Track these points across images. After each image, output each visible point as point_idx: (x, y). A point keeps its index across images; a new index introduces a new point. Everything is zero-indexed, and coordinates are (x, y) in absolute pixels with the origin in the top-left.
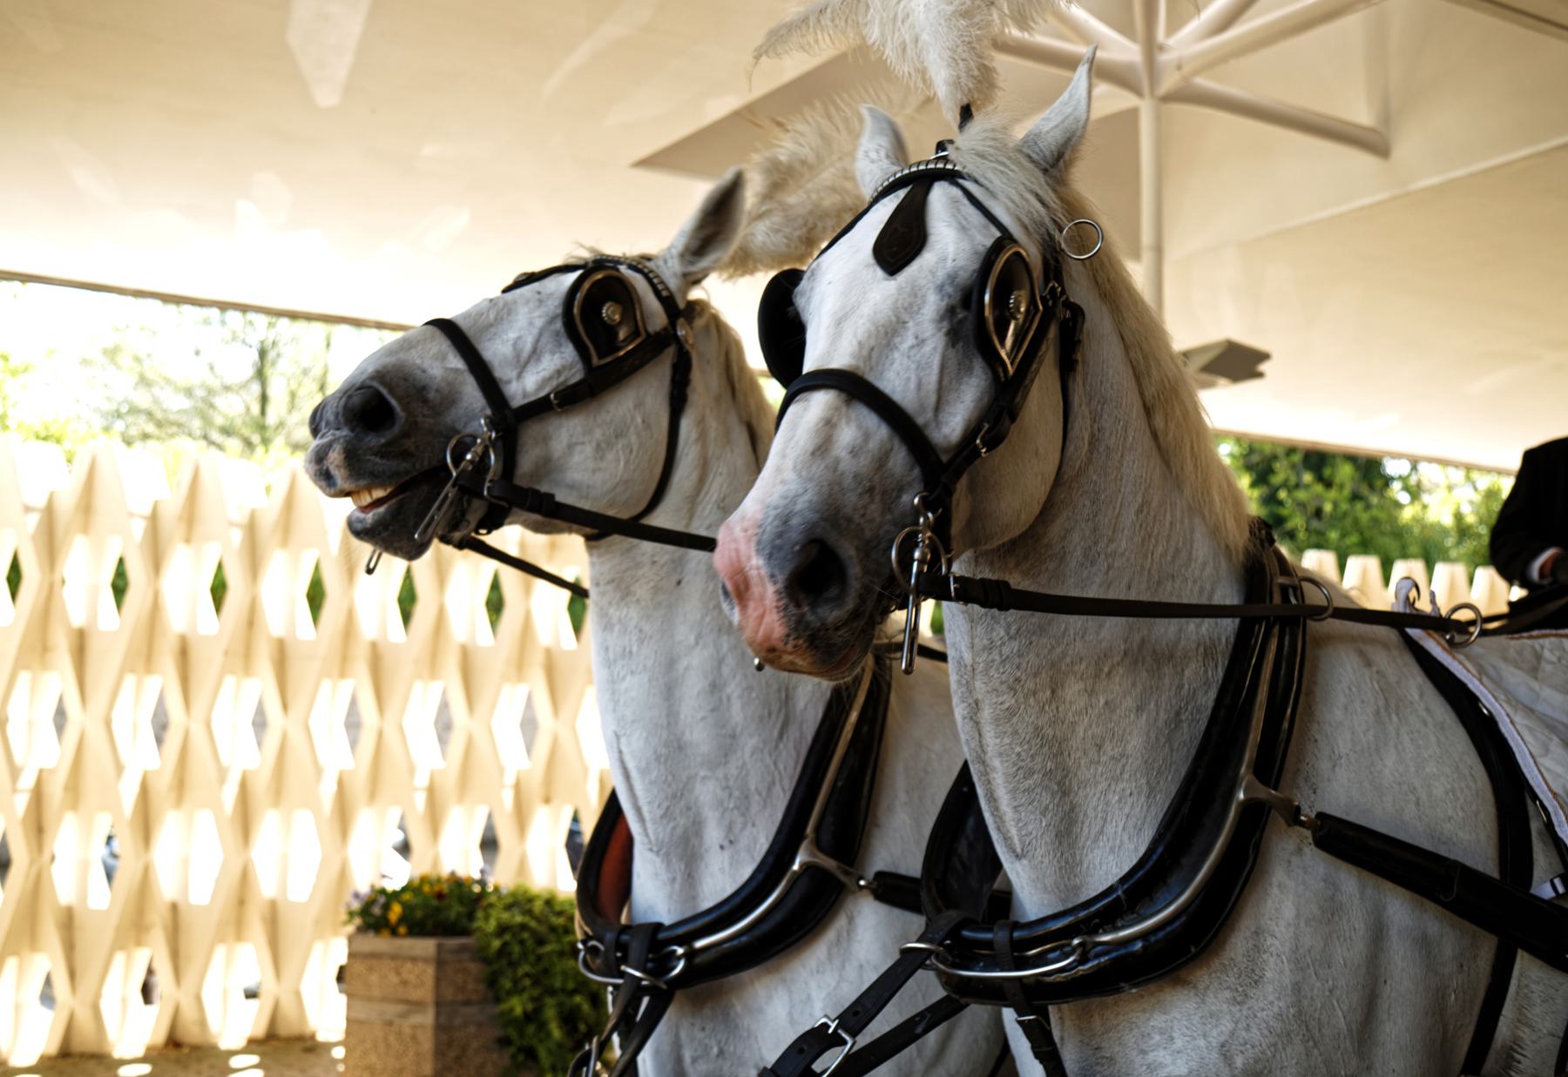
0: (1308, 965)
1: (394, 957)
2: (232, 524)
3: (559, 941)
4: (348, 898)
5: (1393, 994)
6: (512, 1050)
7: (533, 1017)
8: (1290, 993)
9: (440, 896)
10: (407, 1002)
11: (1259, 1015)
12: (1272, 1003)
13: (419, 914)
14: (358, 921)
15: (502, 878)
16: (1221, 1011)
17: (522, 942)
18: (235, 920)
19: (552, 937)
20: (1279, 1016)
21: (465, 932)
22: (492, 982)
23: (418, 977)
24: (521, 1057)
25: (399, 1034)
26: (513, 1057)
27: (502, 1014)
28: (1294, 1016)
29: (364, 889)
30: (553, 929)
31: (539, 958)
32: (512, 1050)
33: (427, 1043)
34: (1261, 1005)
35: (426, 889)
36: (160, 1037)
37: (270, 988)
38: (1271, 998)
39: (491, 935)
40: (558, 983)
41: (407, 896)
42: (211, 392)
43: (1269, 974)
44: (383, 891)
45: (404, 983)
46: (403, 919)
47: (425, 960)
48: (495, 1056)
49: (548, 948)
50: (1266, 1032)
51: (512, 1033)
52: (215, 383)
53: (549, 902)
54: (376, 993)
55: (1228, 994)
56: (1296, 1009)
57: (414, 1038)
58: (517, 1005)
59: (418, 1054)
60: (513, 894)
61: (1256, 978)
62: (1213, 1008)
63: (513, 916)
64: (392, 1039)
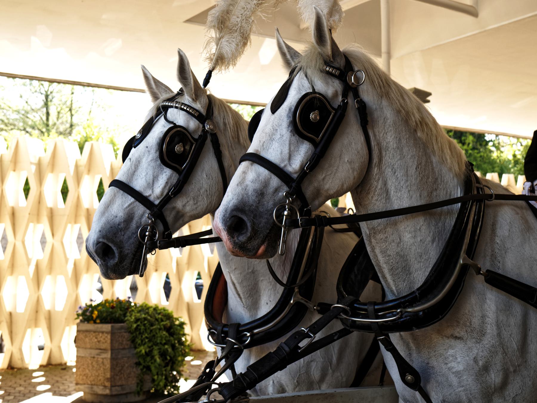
0: (502, 326)
1: (95, 332)
2: (31, 163)
3: (159, 324)
4: (78, 309)
5: (533, 334)
6: (141, 367)
7: (149, 354)
8: (496, 337)
9: (113, 307)
10: (100, 349)
11: (486, 346)
12: (490, 341)
13: (105, 315)
14: (81, 318)
15: (139, 300)
16: (473, 346)
17: (144, 325)
18: (34, 321)
19: (157, 323)
20: (493, 346)
21: (123, 321)
22: (133, 341)
23: (104, 339)
24: (145, 370)
25: (97, 361)
26: (142, 370)
27: (137, 353)
28: (498, 345)
29: (84, 305)
30: (157, 320)
31: (151, 331)
32: (141, 367)
33: (108, 366)
34: (486, 342)
35: (107, 304)
36: (5, 366)
37: (48, 345)
38: (490, 340)
39: (132, 322)
40: (159, 341)
41: (100, 308)
42: (27, 112)
43: (488, 331)
44: (91, 306)
45: (99, 342)
46: (98, 317)
47: (107, 333)
48: (134, 370)
49: (154, 327)
50: (489, 352)
51: (142, 362)
52: (28, 108)
53: (156, 309)
54: (88, 346)
55: (474, 340)
56: (499, 343)
57: (103, 363)
58: (143, 350)
59: (104, 369)
60: (141, 306)
61: (484, 333)
62: (470, 346)
63: (141, 315)
64: (94, 363)
